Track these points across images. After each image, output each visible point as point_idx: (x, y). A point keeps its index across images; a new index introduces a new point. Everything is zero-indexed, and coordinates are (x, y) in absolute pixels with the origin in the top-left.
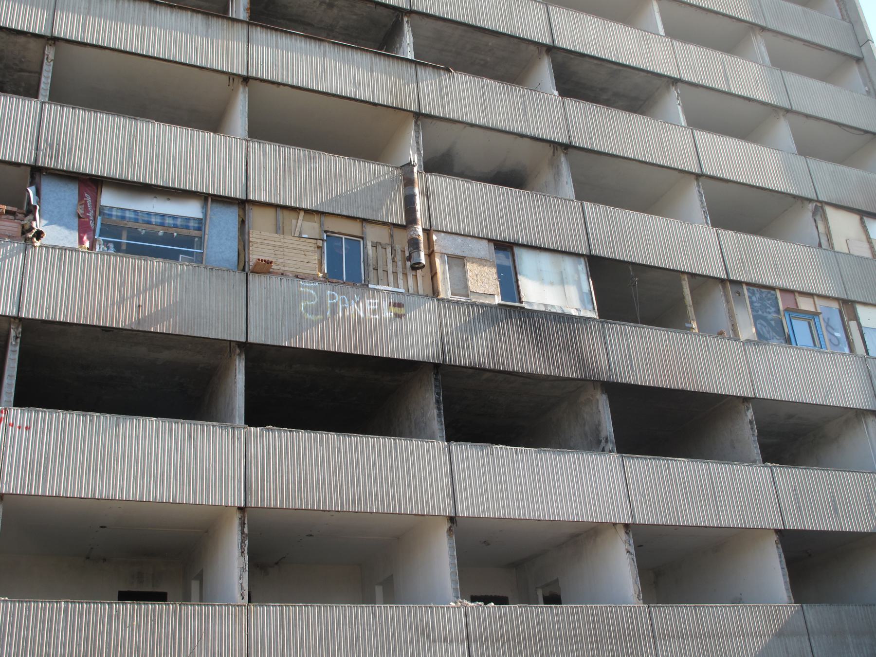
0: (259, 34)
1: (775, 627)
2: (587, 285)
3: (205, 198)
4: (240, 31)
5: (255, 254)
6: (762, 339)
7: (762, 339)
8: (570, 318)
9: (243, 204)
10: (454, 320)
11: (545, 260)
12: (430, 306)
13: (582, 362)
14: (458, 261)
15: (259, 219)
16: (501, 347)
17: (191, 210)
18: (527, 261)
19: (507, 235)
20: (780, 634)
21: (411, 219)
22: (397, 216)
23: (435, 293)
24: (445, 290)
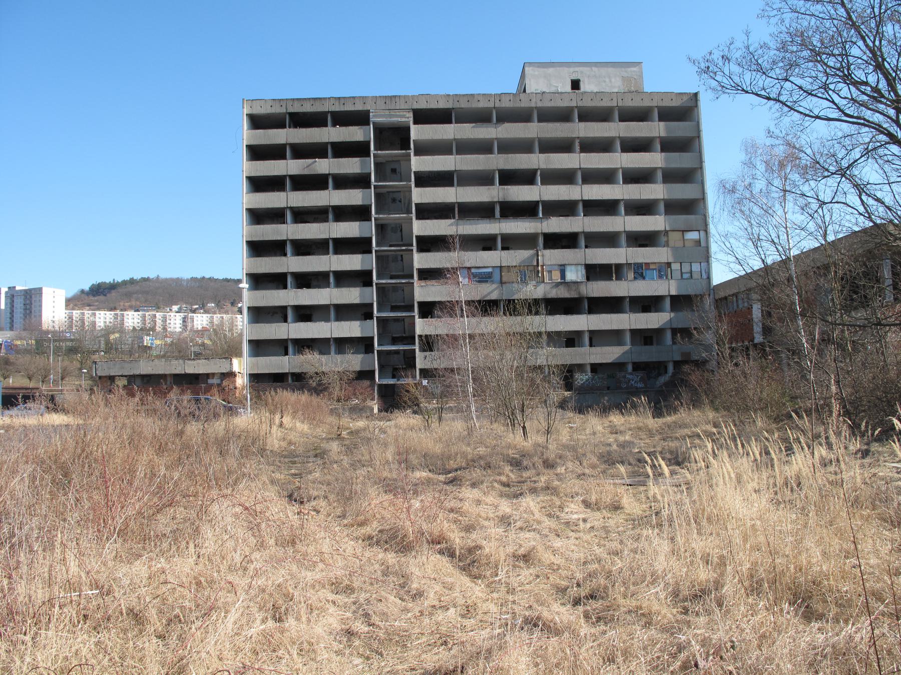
0: (502, 220)
1: (622, 352)
2: (584, 272)
3: (493, 267)
4: (498, 221)
5: (504, 279)
6: (635, 278)
7: (635, 278)
8: (578, 282)
9: (501, 267)
10: (548, 287)
11: (573, 268)
12: (543, 284)
13: (579, 293)
14: (550, 272)
15: (504, 269)
16: (559, 292)
17: (490, 270)
18: (568, 269)
19: (563, 263)
20: (624, 353)
21: (538, 265)
22: (535, 264)
23: (543, 282)
24: (547, 280)
